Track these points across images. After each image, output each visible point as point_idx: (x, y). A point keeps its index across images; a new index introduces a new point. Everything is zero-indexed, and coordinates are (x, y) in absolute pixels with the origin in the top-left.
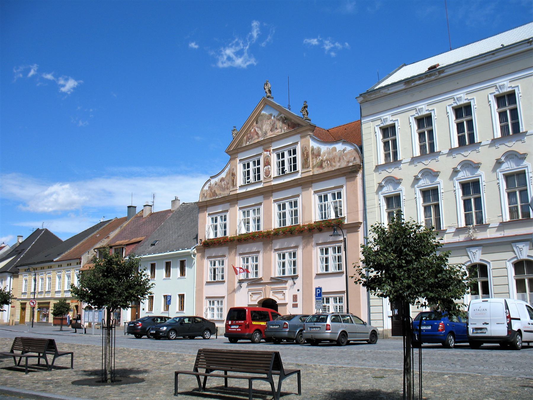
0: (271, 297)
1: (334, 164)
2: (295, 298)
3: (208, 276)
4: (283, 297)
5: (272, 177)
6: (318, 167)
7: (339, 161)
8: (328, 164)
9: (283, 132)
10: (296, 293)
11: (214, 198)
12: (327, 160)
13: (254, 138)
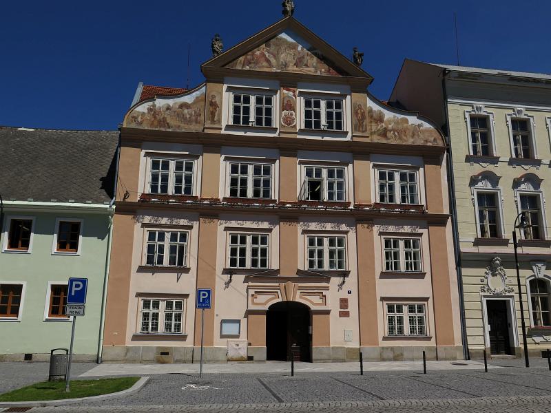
0: (298, 300)
1: (405, 138)
2: (344, 303)
3: (139, 256)
4: (321, 301)
5: (298, 128)
6: (379, 135)
7: (413, 137)
8: (395, 136)
9: (319, 73)
10: (346, 296)
11: (162, 129)
12: (394, 130)
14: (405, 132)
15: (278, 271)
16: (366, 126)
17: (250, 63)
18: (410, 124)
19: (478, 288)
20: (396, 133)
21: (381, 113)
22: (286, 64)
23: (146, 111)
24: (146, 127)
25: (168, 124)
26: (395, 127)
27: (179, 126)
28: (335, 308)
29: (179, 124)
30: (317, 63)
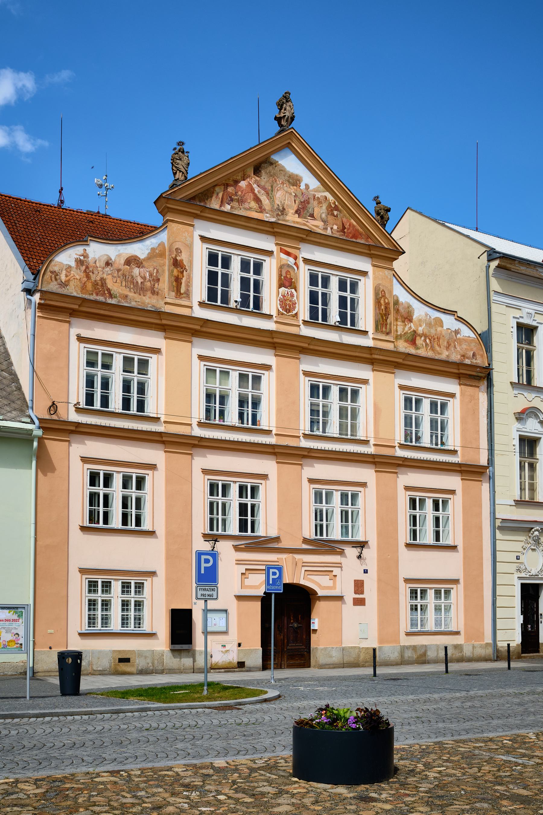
0: (303, 582)
1: (438, 348)
2: (359, 586)
4: (331, 583)
6: (406, 341)
7: (448, 348)
8: (427, 344)
9: (329, 232)
10: (361, 576)
13: (246, 205)
14: (439, 339)
15: (277, 539)
16: (391, 324)
17: (232, 200)
18: (445, 328)
19: (514, 567)
20: (428, 341)
21: (409, 306)
22: (284, 209)
23: (73, 264)
24: (73, 290)
25: (109, 290)
26: (426, 331)
27: (126, 296)
28: (350, 595)
29: (126, 292)
30: (327, 216)
